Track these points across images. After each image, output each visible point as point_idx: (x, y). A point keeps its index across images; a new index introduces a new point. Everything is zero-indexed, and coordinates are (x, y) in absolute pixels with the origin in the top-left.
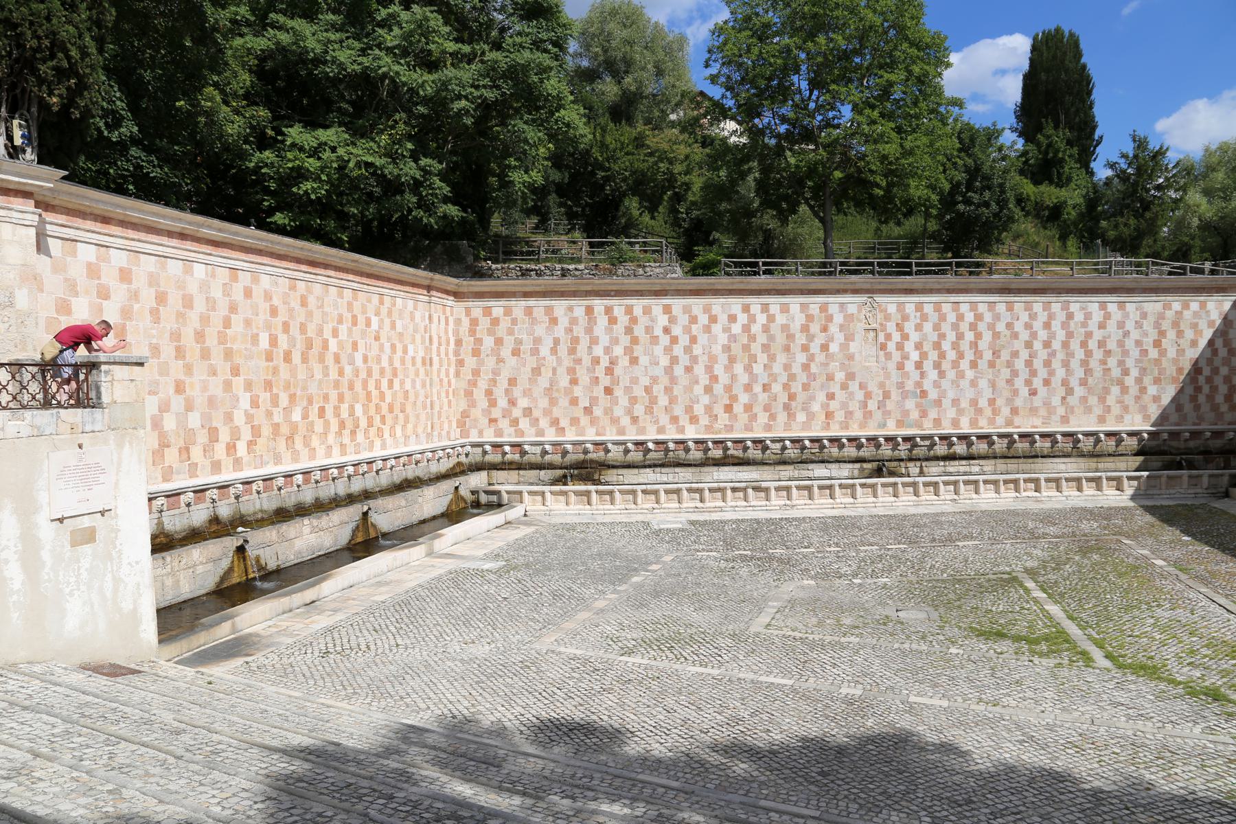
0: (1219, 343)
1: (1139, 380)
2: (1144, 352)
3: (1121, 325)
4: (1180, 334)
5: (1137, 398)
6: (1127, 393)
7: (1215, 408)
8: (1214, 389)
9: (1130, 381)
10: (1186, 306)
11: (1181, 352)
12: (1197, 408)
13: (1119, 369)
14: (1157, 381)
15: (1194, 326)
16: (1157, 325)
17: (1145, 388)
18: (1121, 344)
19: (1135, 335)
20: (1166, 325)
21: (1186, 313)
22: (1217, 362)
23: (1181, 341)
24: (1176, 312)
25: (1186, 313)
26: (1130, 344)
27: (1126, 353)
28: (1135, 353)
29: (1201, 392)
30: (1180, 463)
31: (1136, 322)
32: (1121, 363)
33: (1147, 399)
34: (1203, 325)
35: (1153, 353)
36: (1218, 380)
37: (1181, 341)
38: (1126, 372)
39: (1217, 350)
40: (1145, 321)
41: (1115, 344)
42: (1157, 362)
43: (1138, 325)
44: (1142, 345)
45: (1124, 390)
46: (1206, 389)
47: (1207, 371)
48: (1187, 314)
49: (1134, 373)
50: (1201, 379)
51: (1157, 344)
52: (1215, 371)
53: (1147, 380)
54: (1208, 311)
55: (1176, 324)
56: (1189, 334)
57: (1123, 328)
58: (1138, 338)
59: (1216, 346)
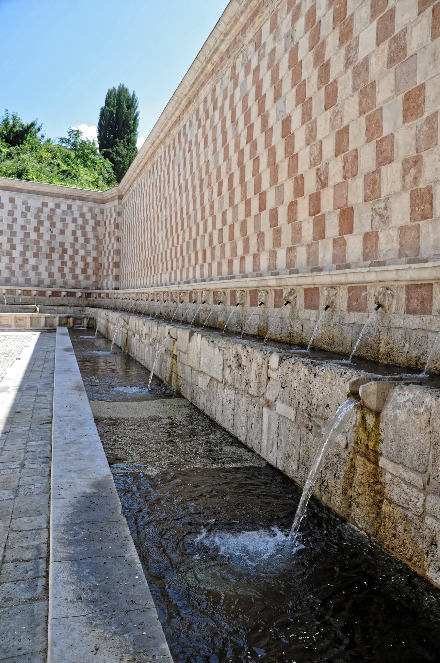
0: (79, 233)
1: (23, 254)
2: (27, 235)
3: (11, 213)
4: (53, 225)
5: (21, 267)
6: (14, 262)
7: (75, 277)
8: (75, 264)
9: (16, 254)
10: (58, 206)
11: (53, 237)
12: (63, 276)
13: (9, 244)
14: (36, 255)
15: (63, 220)
16: (37, 216)
17: (27, 260)
18: (10, 227)
19: (21, 221)
20: (43, 217)
21: (57, 210)
22: (77, 246)
23: (54, 230)
24: (51, 210)
25: (57, 210)
26: (17, 228)
27: (14, 234)
28: (20, 234)
29: (66, 266)
30: (36, 310)
31: (22, 213)
32: (10, 240)
33: (28, 267)
34: (69, 219)
35: (34, 236)
36: (78, 259)
37: (54, 230)
38: (13, 247)
39: (77, 238)
40: (28, 213)
41: (6, 226)
42: (36, 242)
43: (24, 215)
44: (26, 230)
45: (12, 260)
46: (69, 264)
47: (70, 252)
48: (59, 212)
49: (20, 248)
50: (67, 257)
51: (36, 229)
52: (76, 252)
53: (29, 254)
54: (72, 212)
55: (50, 218)
56: (59, 225)
57: (13, 215)
58: (23, 224)
59: (77, 235)
